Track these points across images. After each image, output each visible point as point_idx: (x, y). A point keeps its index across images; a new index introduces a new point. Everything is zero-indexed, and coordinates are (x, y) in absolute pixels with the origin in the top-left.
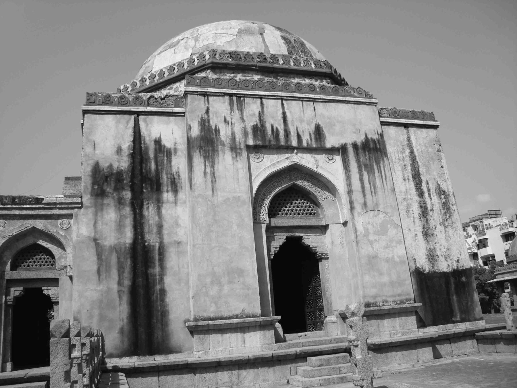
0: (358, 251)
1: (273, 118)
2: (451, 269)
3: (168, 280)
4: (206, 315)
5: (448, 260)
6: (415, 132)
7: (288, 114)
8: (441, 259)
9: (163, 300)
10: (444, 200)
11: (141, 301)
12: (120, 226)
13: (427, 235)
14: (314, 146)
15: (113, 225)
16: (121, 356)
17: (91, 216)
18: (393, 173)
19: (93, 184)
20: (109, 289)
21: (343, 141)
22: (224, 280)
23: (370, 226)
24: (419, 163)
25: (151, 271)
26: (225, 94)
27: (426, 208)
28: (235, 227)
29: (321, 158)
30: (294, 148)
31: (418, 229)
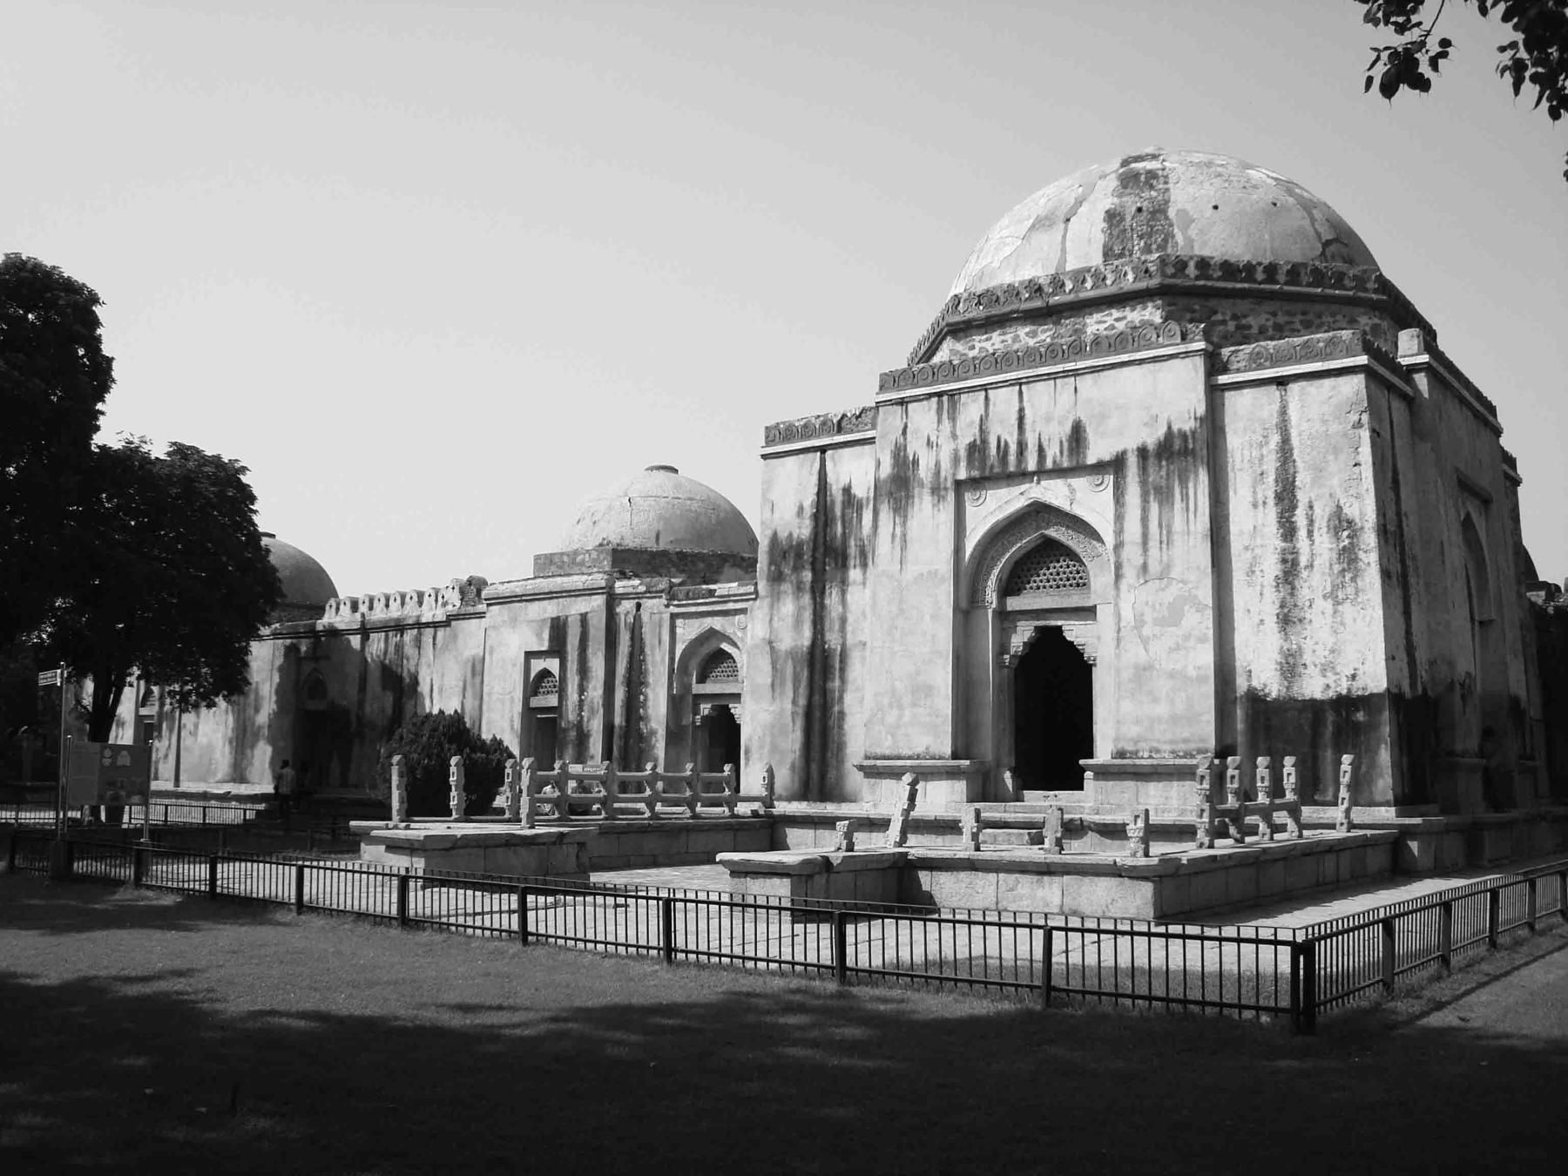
0: (1118, 656)
1: (1001, 422)
2: (1331, 694)
3: (849, 698)
4: (879, 751)
5: (1329, 674)
6: (1302, 392)
7: (1027, 412)
8: (1311, 670)
9: (841, 727)
10: (1347, 542)
11: (817, 727)
12: (798, 622)
13: (1287, 620)
14: (1066, 465)
15: (790, 621)
16: (790, 799)
17: (766, 610)
18: (1389, 454)
19: (770, 564)
20: (783, 710)
21: (1120, 448)
22: (907, 700)
23: (1147, 610)
24: (1299, 464)
25: (830, 685)
26: (930, 395)
27: (1295, 563)
28: (927, 618)
29: (1081, 483)
30: (1034, 473)
31: (1269, 608)
